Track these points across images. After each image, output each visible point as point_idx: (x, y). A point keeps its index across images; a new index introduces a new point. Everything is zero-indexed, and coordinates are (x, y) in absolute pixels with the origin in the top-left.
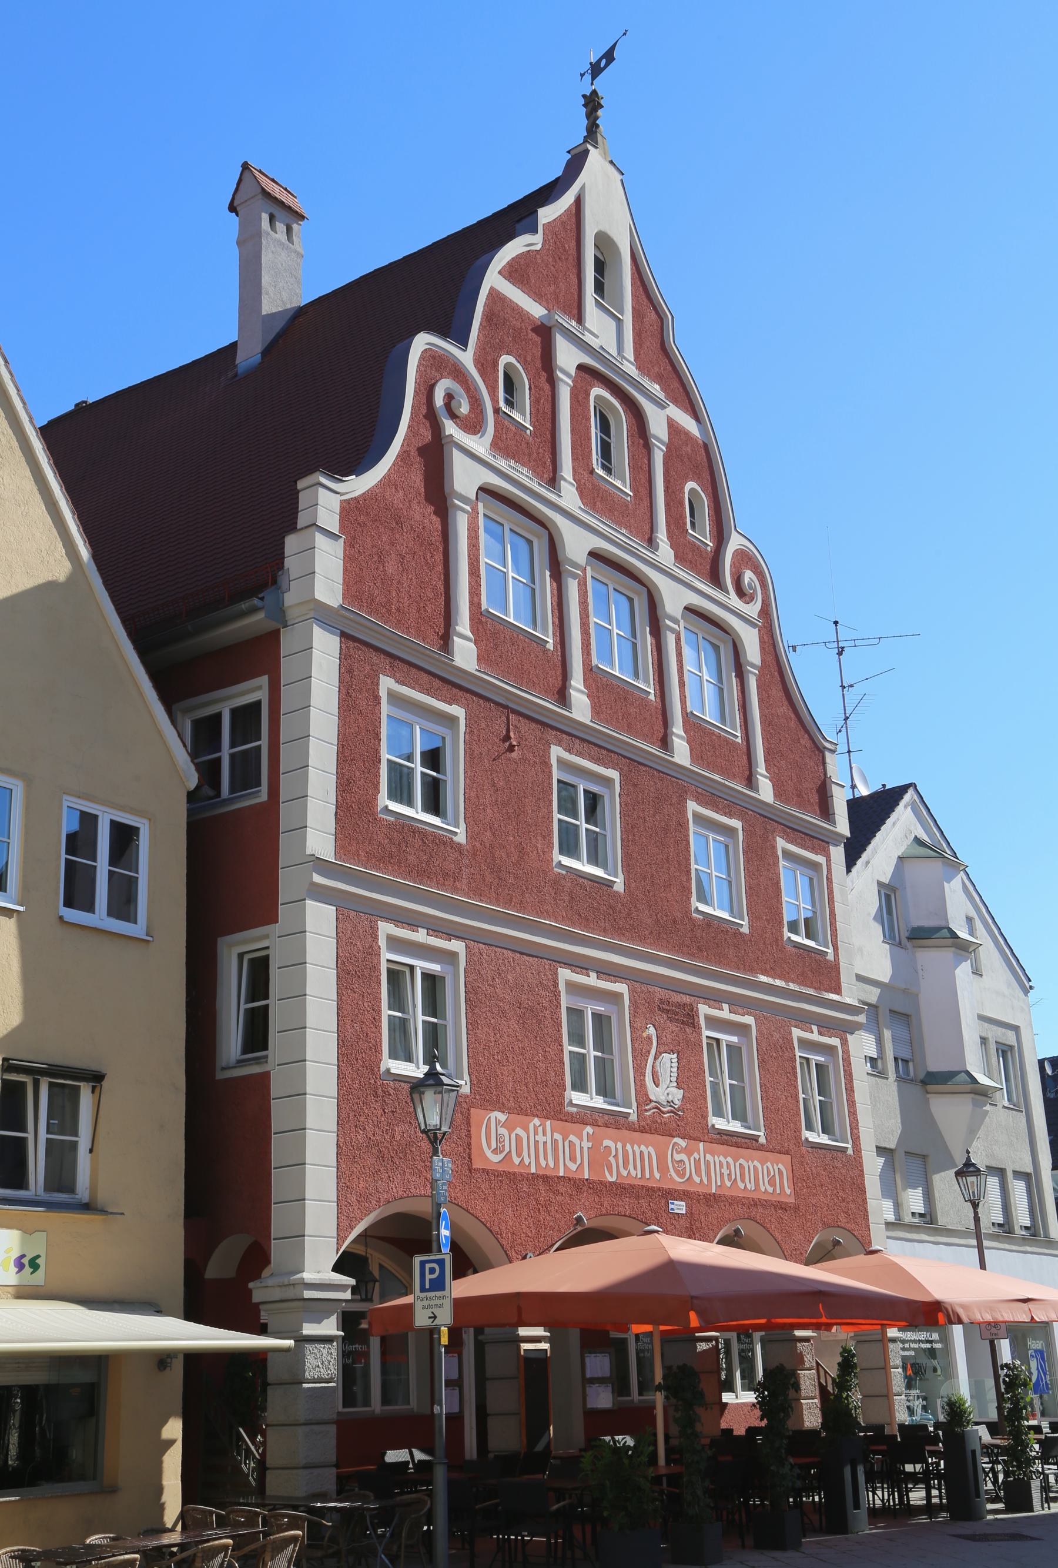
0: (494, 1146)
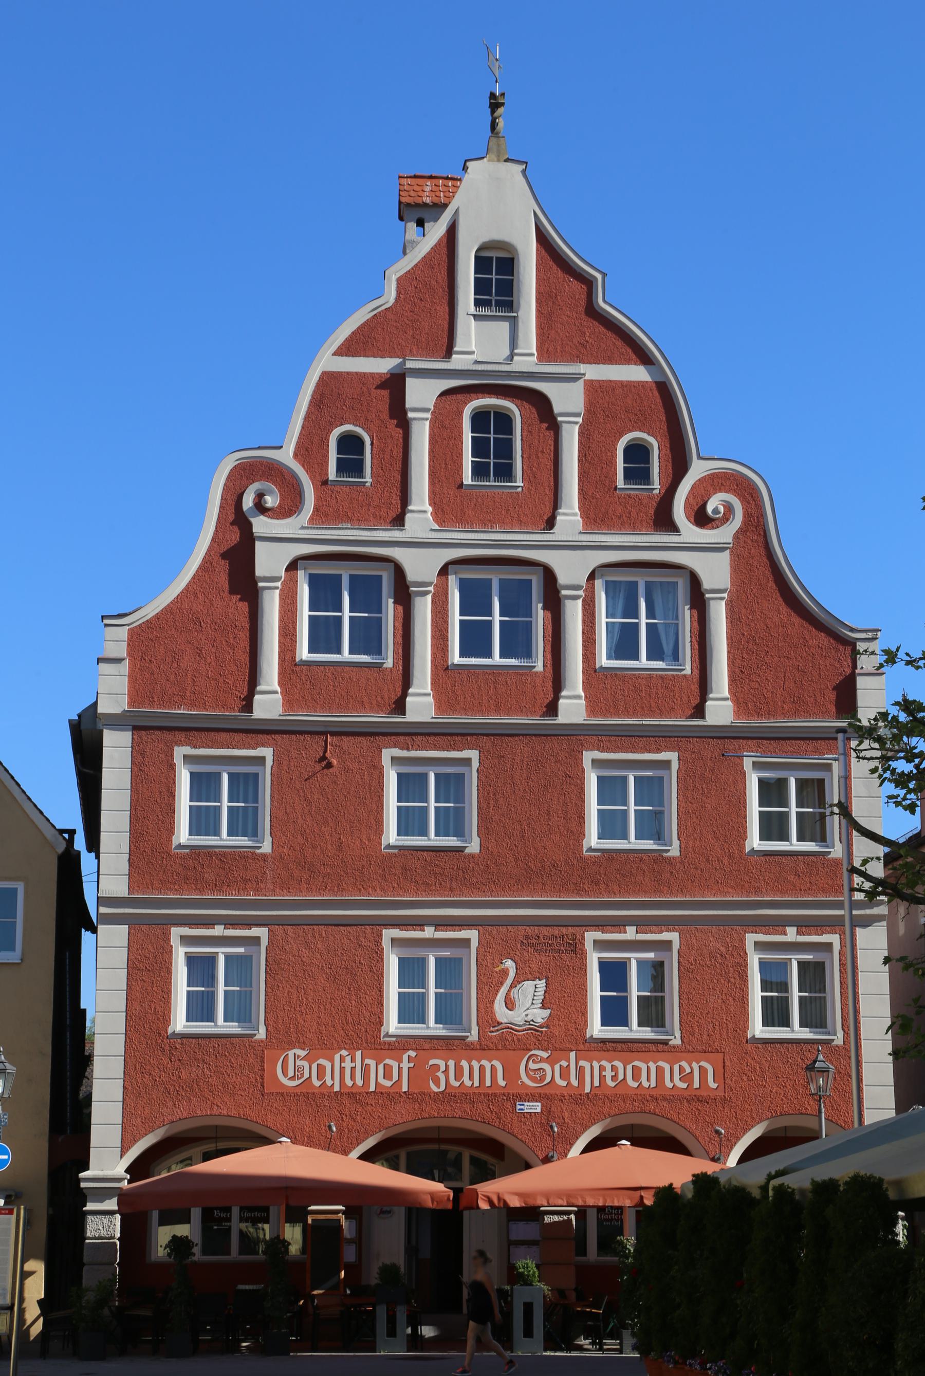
0: (291, 1074)
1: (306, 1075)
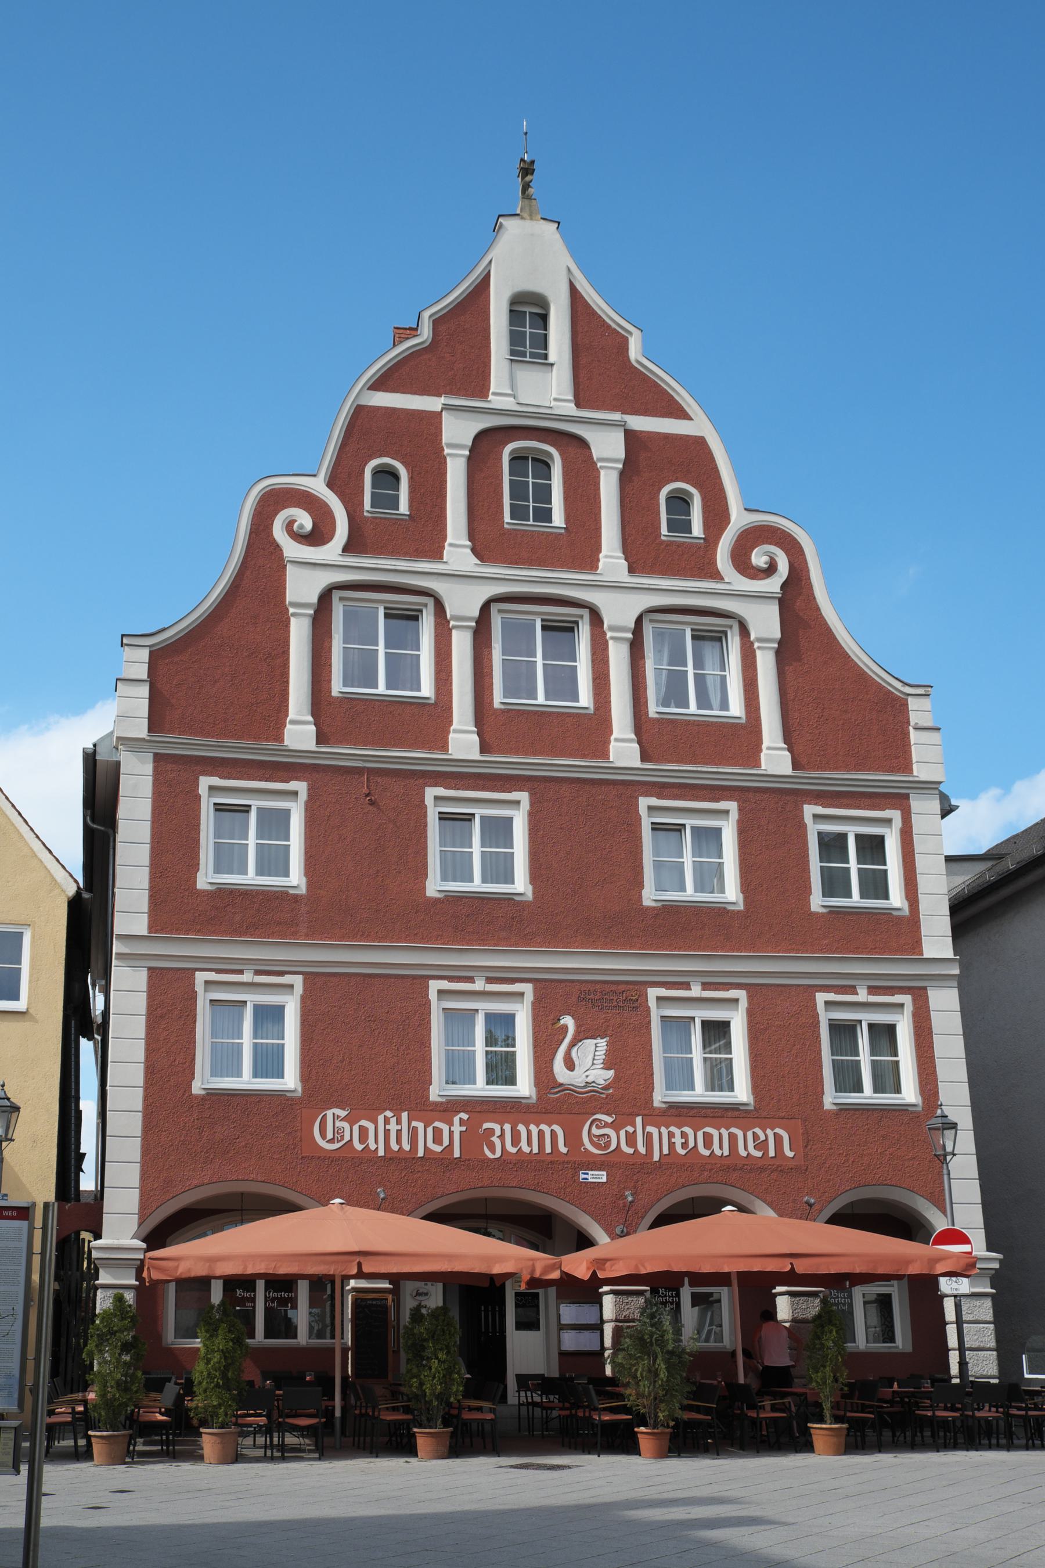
0: (330, 1136)
1: (347, 1138)
